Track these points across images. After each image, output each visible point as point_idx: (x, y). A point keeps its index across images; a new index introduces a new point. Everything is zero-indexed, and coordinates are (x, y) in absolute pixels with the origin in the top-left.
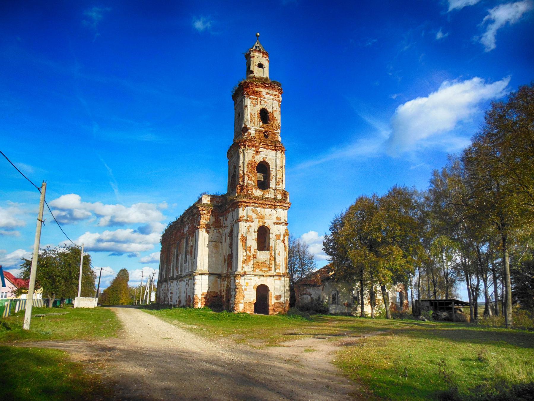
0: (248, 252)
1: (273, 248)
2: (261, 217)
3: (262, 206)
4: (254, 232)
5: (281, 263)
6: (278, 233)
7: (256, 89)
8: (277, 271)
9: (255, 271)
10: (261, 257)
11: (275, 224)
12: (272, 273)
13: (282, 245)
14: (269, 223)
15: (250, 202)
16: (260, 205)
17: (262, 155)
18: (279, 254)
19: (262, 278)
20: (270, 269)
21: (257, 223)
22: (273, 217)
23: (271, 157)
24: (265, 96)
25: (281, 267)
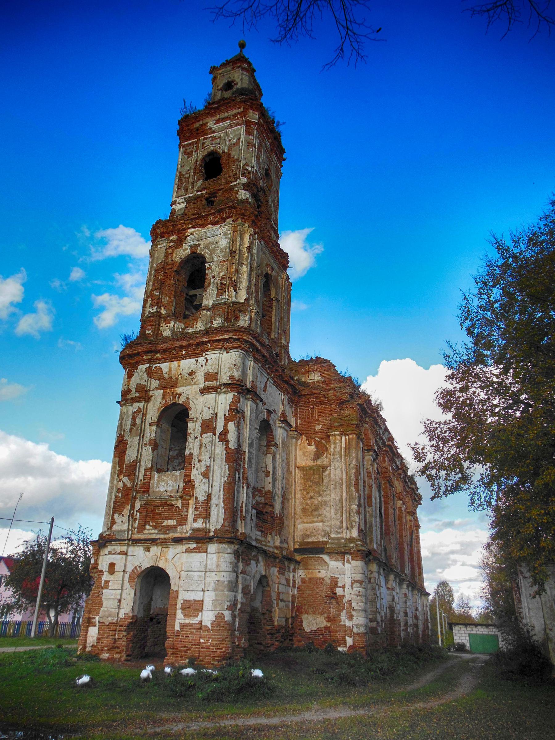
0: (125, 479)
1: (195, 460)
2: (169, 384)
3: (174, 355)
4: (151, 424)
5: (214, 501)
6: (207, 415)
7: (197, 125)
8: (199, 524)
9: (141, 529)
10: (162, 489)
11: (204, 391)
12: (186, 530)
13: (219, 448)
14: (188, 392)
15: (139, 354)
16: (166, 355)
17: (190, 241)
18: (206, 475)
19: (155, 550)
20: (182, 521)
21: (159, 400)
22: (200, 377)
23: (210, 240)
24: (214, 127)
25: (214, 512)
